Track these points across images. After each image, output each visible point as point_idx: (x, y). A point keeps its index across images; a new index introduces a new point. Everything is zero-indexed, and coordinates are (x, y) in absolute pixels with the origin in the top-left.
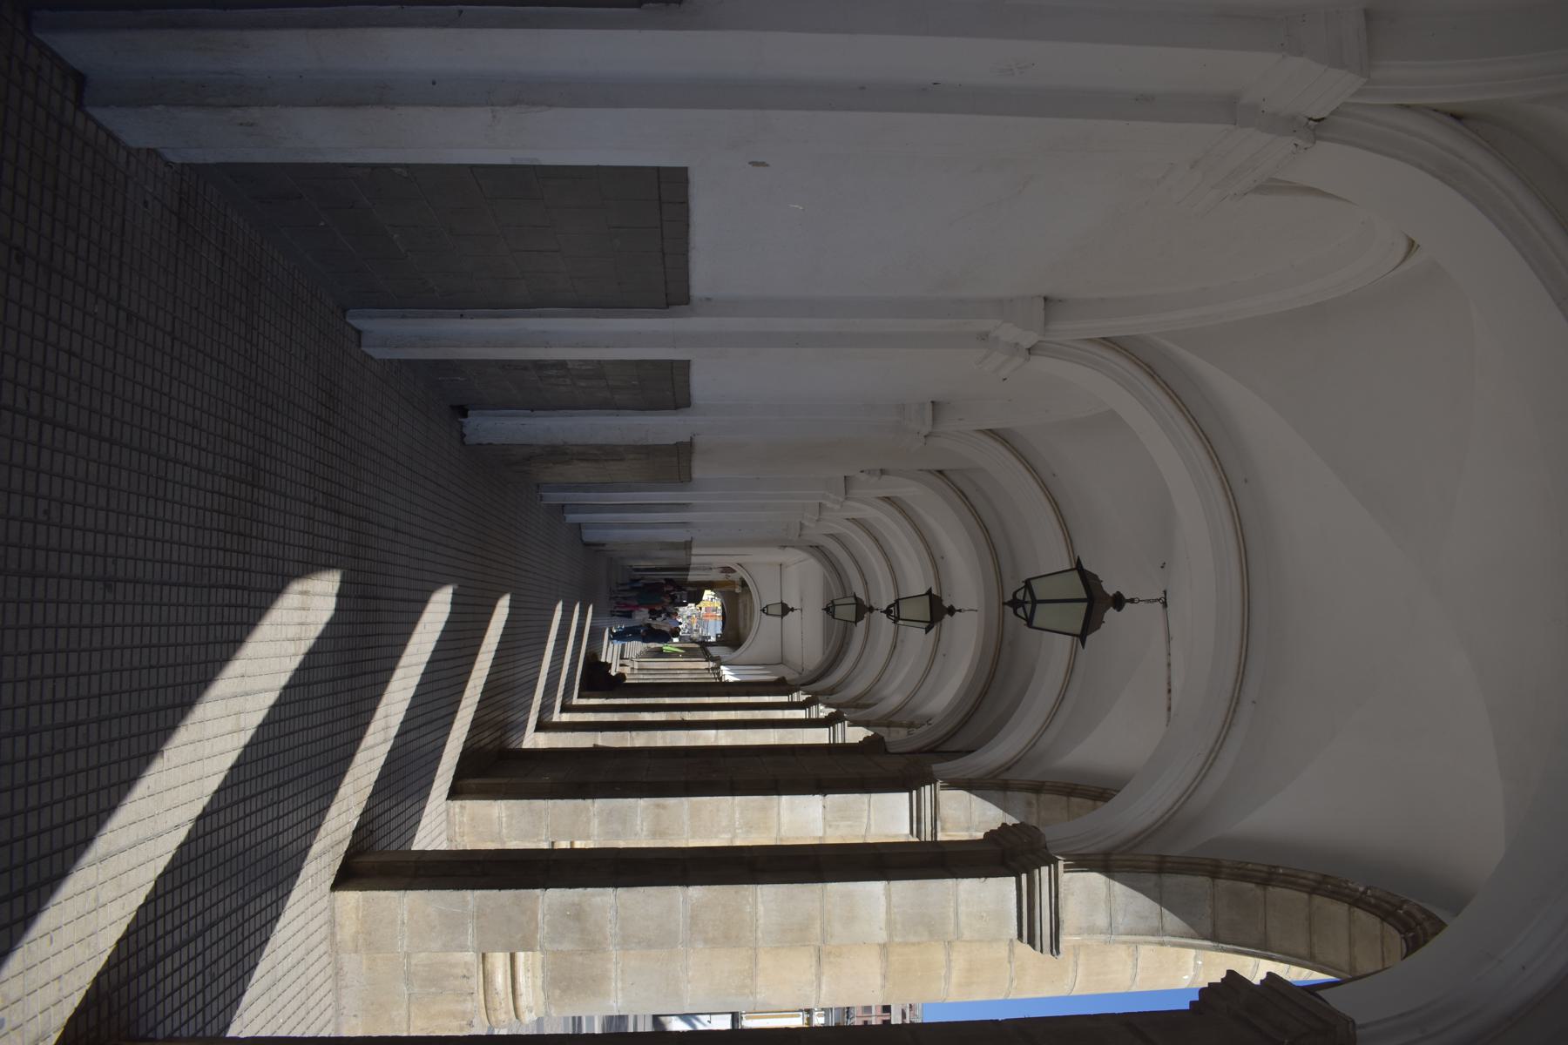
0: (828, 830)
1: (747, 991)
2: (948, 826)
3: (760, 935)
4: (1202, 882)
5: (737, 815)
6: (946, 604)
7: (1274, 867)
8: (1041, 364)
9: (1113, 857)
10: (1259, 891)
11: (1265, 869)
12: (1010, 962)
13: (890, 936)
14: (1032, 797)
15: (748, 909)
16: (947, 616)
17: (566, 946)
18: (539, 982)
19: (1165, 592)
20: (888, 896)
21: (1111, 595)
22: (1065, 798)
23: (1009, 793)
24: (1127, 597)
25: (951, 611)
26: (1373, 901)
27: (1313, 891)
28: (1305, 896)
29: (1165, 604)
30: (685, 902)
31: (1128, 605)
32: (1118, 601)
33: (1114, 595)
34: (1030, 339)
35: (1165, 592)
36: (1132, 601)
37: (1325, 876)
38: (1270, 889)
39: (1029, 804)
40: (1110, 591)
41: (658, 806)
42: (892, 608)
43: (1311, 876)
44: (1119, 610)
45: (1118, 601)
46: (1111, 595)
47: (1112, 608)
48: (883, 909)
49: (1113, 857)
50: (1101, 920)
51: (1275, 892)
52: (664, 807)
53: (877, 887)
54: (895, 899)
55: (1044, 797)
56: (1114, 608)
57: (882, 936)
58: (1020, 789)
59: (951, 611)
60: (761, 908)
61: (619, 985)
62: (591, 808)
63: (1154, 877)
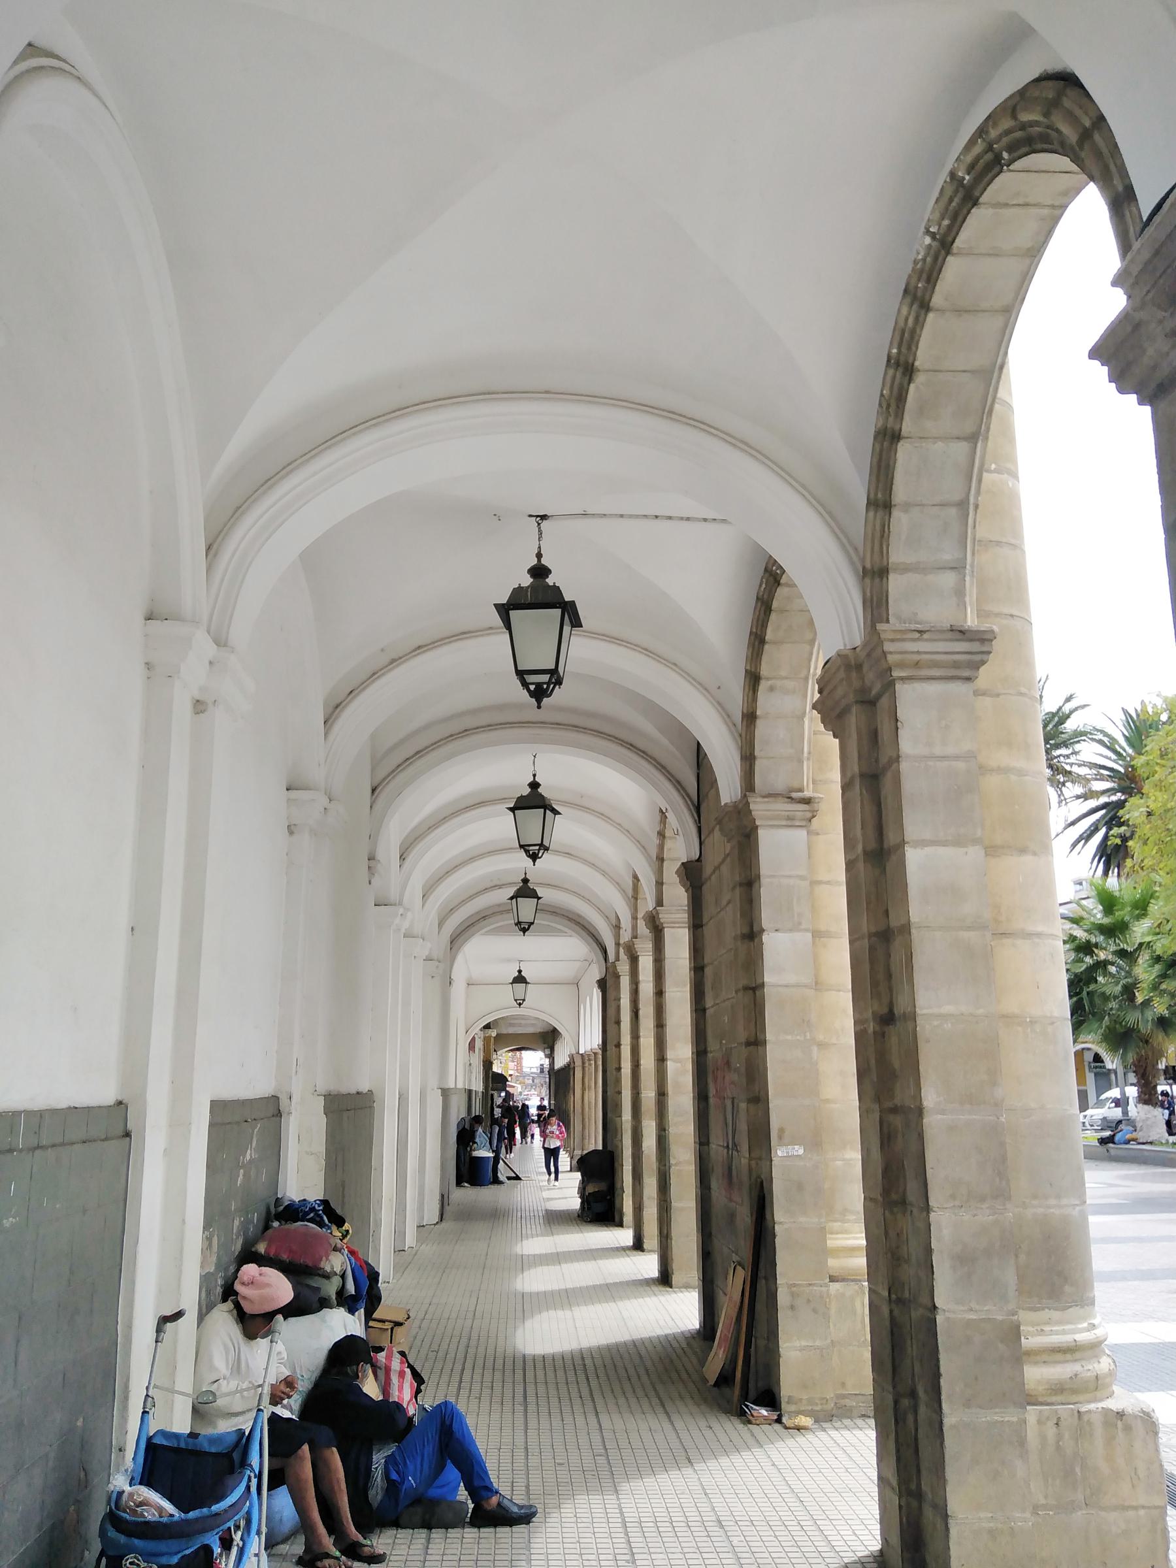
0: (803, 927)
1: (1050, 1029)
2: (796, 785)
3: (981, 1011)
4: (904, 453)
5: (789, 1037)
6: (527, 791)
7: (889, 361)
8: (241, 631)
9: (868, 566)
10: (920, 379)
11: (891, 372)
12: (998, 695)
13: (976, 841)
14: (763, 686)
15: (948, 1026)
17: (1010, 1277)
18: (1056, 1315)
19: (530, 516)
20: (923, 843)
21: (532, 580)
22: (766, 647)
23: (758, 713)
24: (535, 561)
25: (534, 785)
26: (946, 222)
27: (925, 306)
28: (931, 316)
29: (544, 517)
30: (943, 1112)
31: (543, 561)
32: (539, 572)
33: (531, 576)
34: (203, 645)
35: (530, 516)
36: (539, 556)
37: (906, 291)
38: (917, 364)
39: (772, 689)
40: (527, 581)
41: (780, 1138)
42: (531, 852)
43: (905, 311)
45: (539, 572)
46: (532, 580)
47: (547, 580)
48: (941, 851)
49: (868, 566)
50: (948, 579)
51: (923, 357)
52: (781, 1131)
53: (914, 858)
54: (927, 835)
55: (765, 670)
56: (548, 577)
57: (974, 853)
58: (754, 699)
59: (534, 785)
60: (948, 1009)
61: (1052, 1202)
62: (786, 1226)
63: (896, 513)
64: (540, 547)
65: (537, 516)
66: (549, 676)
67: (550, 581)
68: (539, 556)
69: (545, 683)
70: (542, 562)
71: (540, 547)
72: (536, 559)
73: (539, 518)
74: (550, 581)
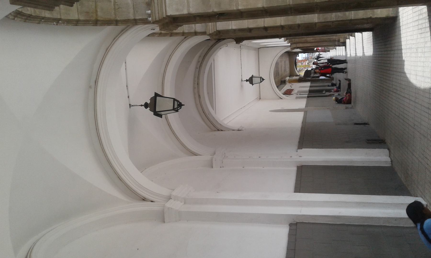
16: (248, 79)
19: (130, 108)
24: (143, 107)
31: (143, 104)
32: (146, 105)
35: (130, 108)
36: (142, 105)
44: (147, 102)
45: (146, 105)
64: (139, 106)
65: (130, 106)
66: (175, 101)
67: (149, 102)
68: (142, 105)
69: (178, 103)
70: (144, 105)
72: (143, 106)
73: (131, 106)
74: (149, 102)
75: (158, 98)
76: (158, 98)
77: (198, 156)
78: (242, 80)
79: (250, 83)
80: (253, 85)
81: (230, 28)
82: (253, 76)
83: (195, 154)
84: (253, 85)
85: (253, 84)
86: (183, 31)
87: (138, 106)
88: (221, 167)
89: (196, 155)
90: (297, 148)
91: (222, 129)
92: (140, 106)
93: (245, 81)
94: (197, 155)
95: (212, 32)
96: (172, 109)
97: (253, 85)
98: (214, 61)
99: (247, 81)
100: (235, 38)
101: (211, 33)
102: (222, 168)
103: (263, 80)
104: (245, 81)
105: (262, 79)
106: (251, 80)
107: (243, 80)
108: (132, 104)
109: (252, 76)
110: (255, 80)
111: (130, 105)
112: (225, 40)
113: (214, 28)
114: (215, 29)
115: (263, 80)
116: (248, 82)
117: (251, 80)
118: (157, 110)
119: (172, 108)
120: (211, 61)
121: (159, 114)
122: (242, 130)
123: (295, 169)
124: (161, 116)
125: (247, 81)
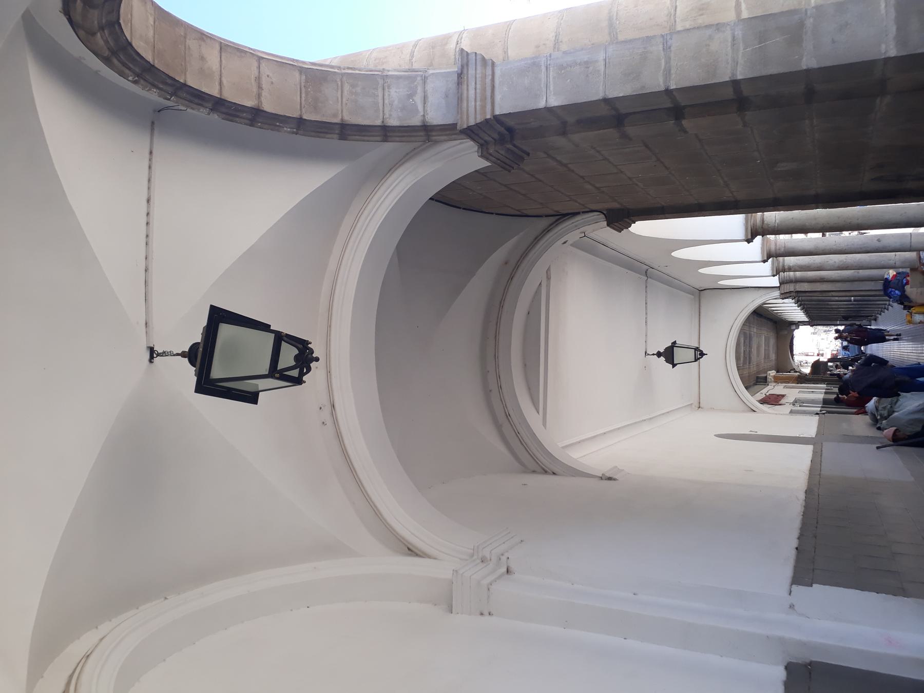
6: (662, 359)
16: (662, 351)
64: (178, 355)
71: (178, 355)
75: (226, 331)
76: (226, 331)
77: (424, 557)
78: (646, 353)
79: (667, 361)
80: (674, 365)
81: (542, 104)
82: (675, 343)
83: (411, 551)
84: (673, 367)
85: (675, 363)
86: (383, 122)
87: (174, 355)
88: (482, 614)
89: (417, 555)
90: (787, 571)
91: (556, 470)
92: (180, 357)
93: (654, 354)
94: (421, 554)
95: (478, 121)
96: (267, 373)
97: (674, 365)
98: (549, 278)
99: (659, 354)
100: (605, 212)
101: (472, 122)
102: (487, 618)
103: (702, 354)
104: (654, 354)
105: (698, 352)
106: (669, 354)
107: (648, 352)
108: (159, 349)
109: (672, 343)
110: (679, 355)
111: (152, 350)
112: (578, 218)
113: (483, 107)
114: (489, 107)
115: (702, 354)
116: (662, 357)
117: (669, 354)
118: (217, 372)
119: (265, 369)
120: (536, 275)
121: (229, 389)
122: (615, 480)
123: (780, 673)
124: (252, 398)
125: (659, 354)
